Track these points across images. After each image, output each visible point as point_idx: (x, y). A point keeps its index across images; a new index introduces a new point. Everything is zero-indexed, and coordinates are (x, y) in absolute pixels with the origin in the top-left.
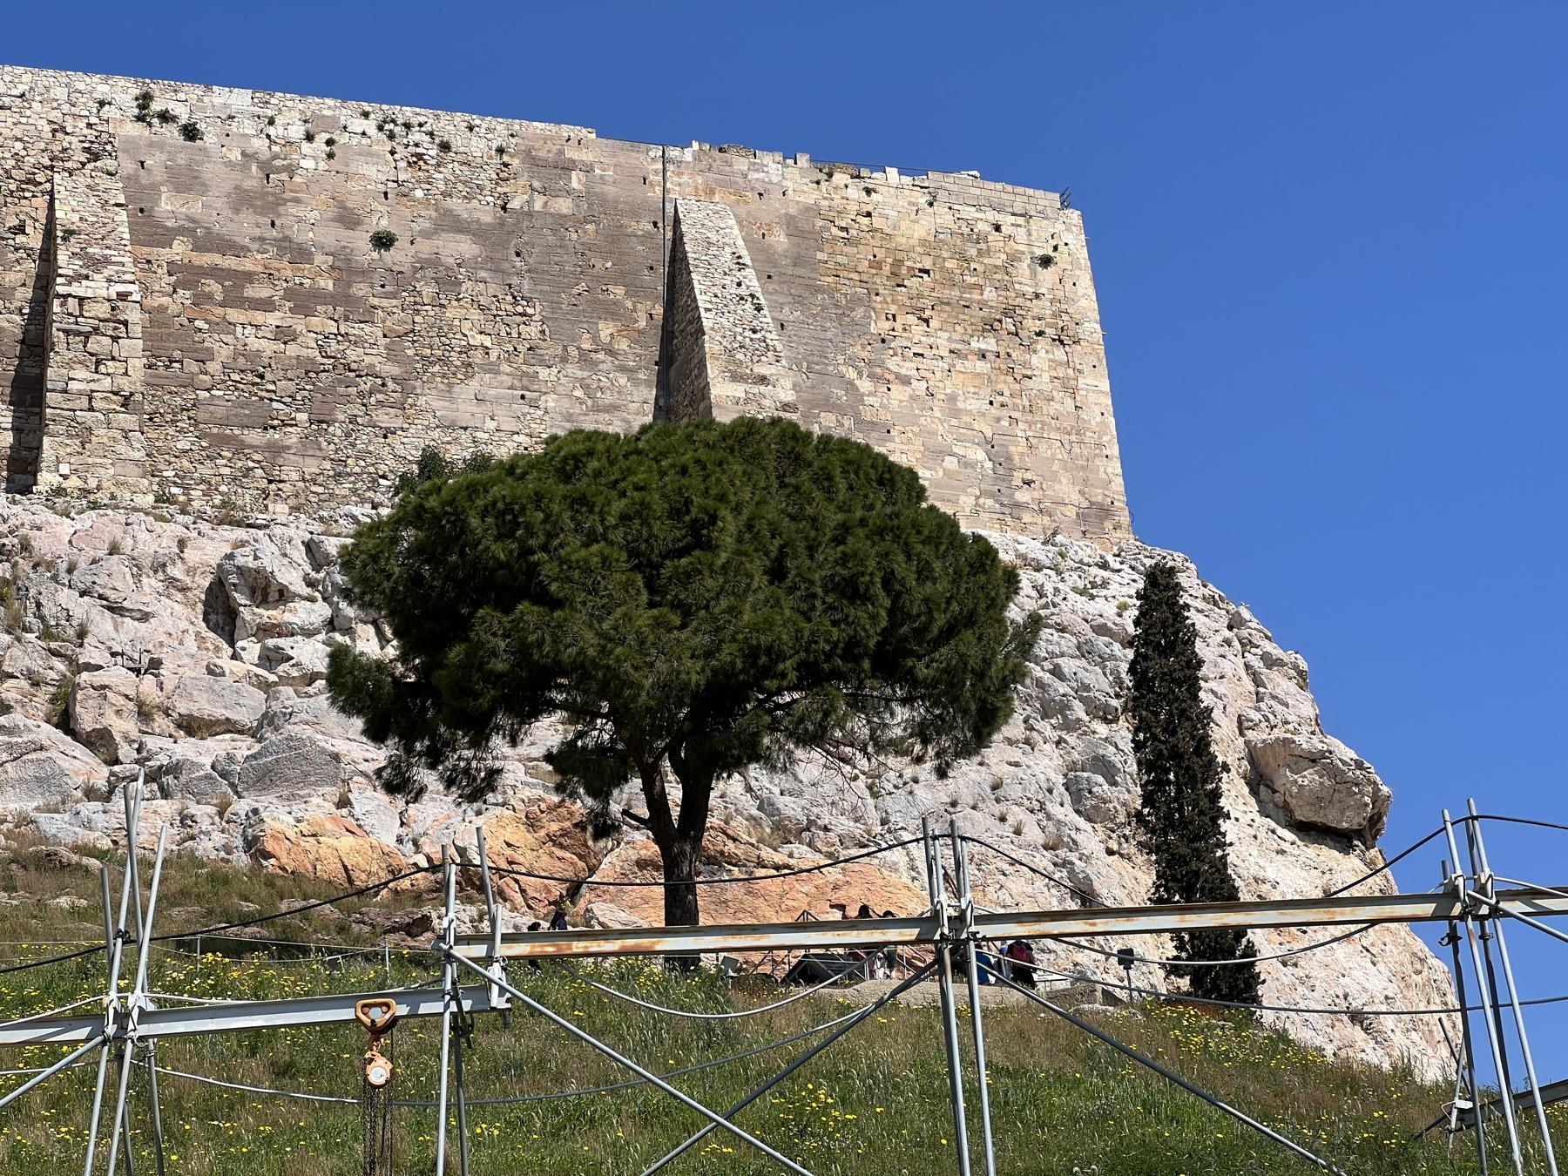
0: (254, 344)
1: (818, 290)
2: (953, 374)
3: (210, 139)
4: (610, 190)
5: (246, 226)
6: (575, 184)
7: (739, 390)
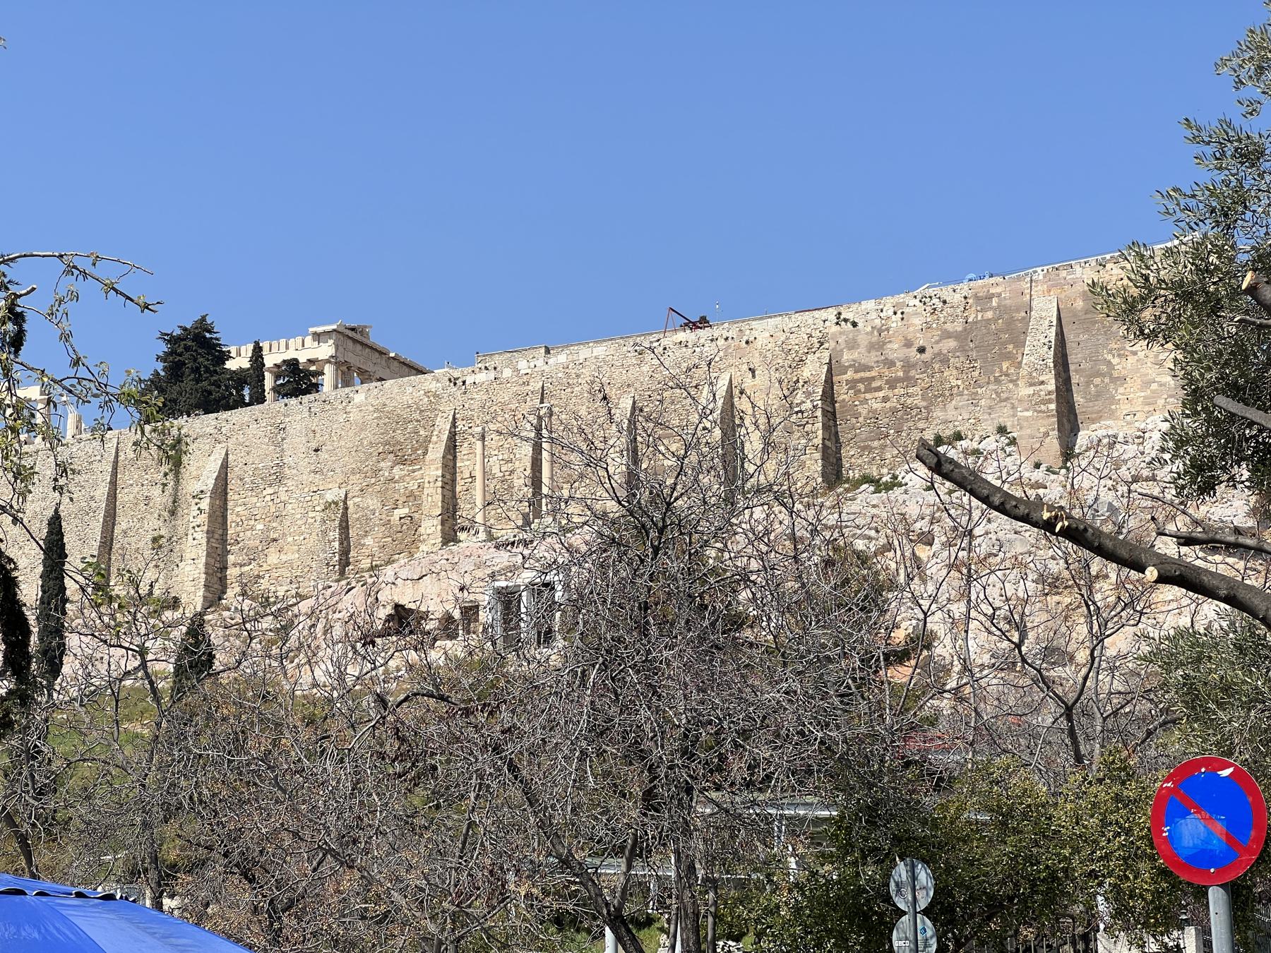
0: (875, 406)
1: (1096, 322)
3: (860, 325)
4: (1008, 302)
5: (873, 357)
6: (994, 304)
7: (1030, 391)
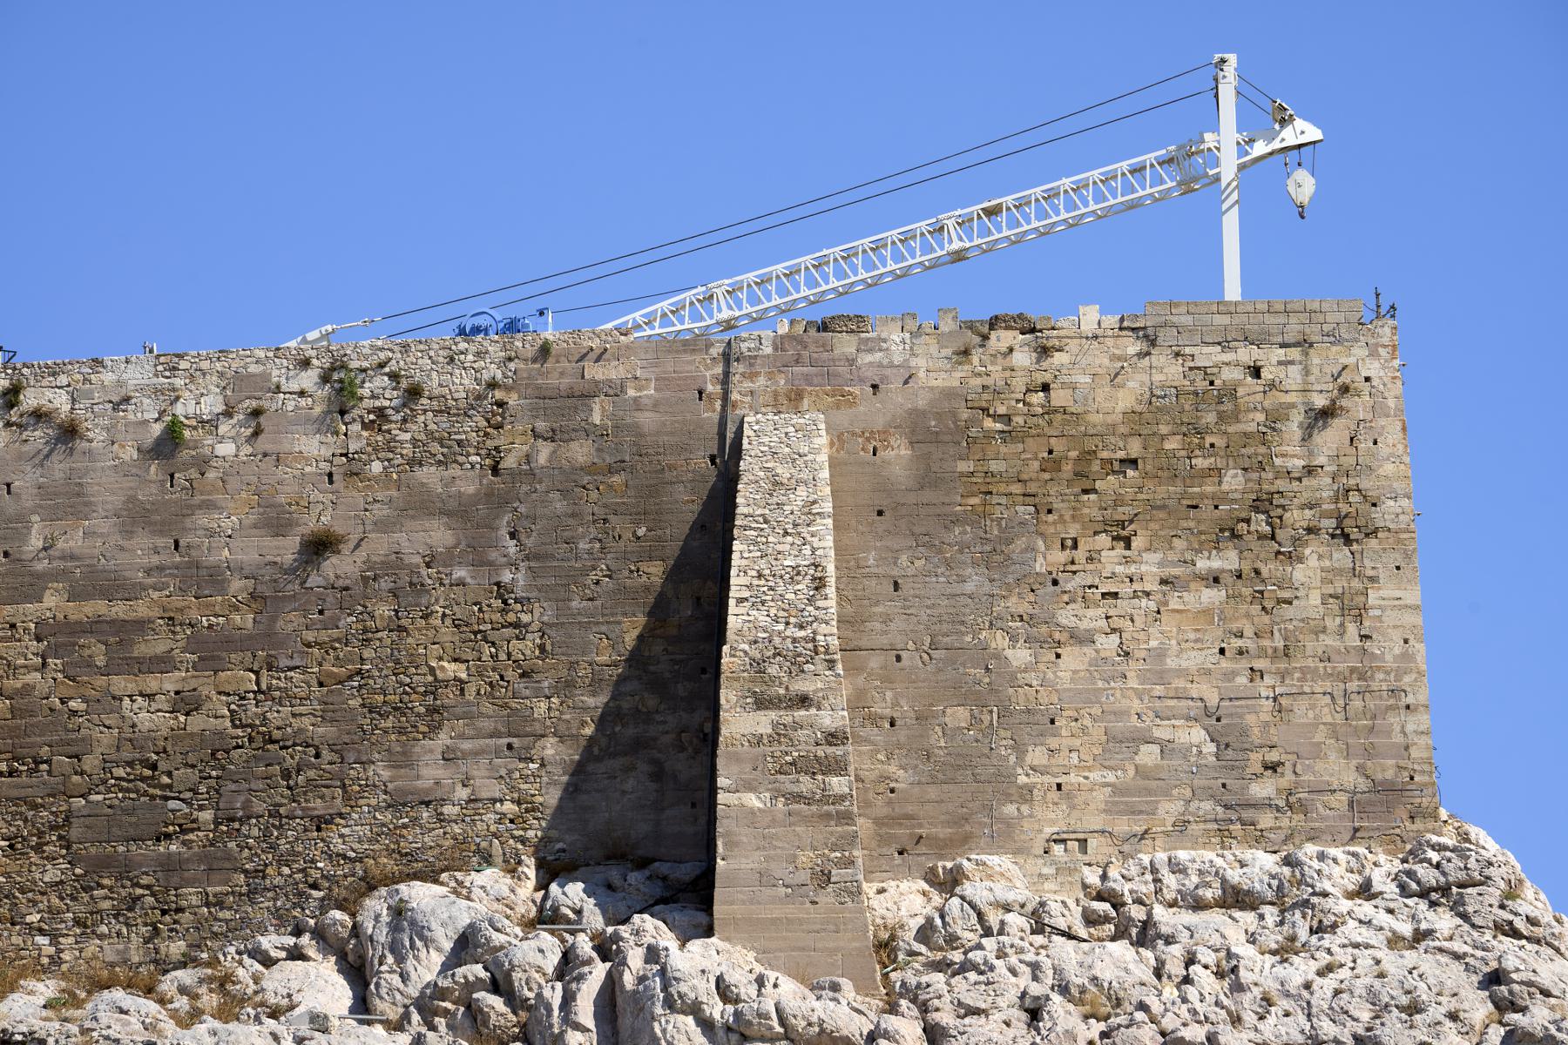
2: (1164, 617)
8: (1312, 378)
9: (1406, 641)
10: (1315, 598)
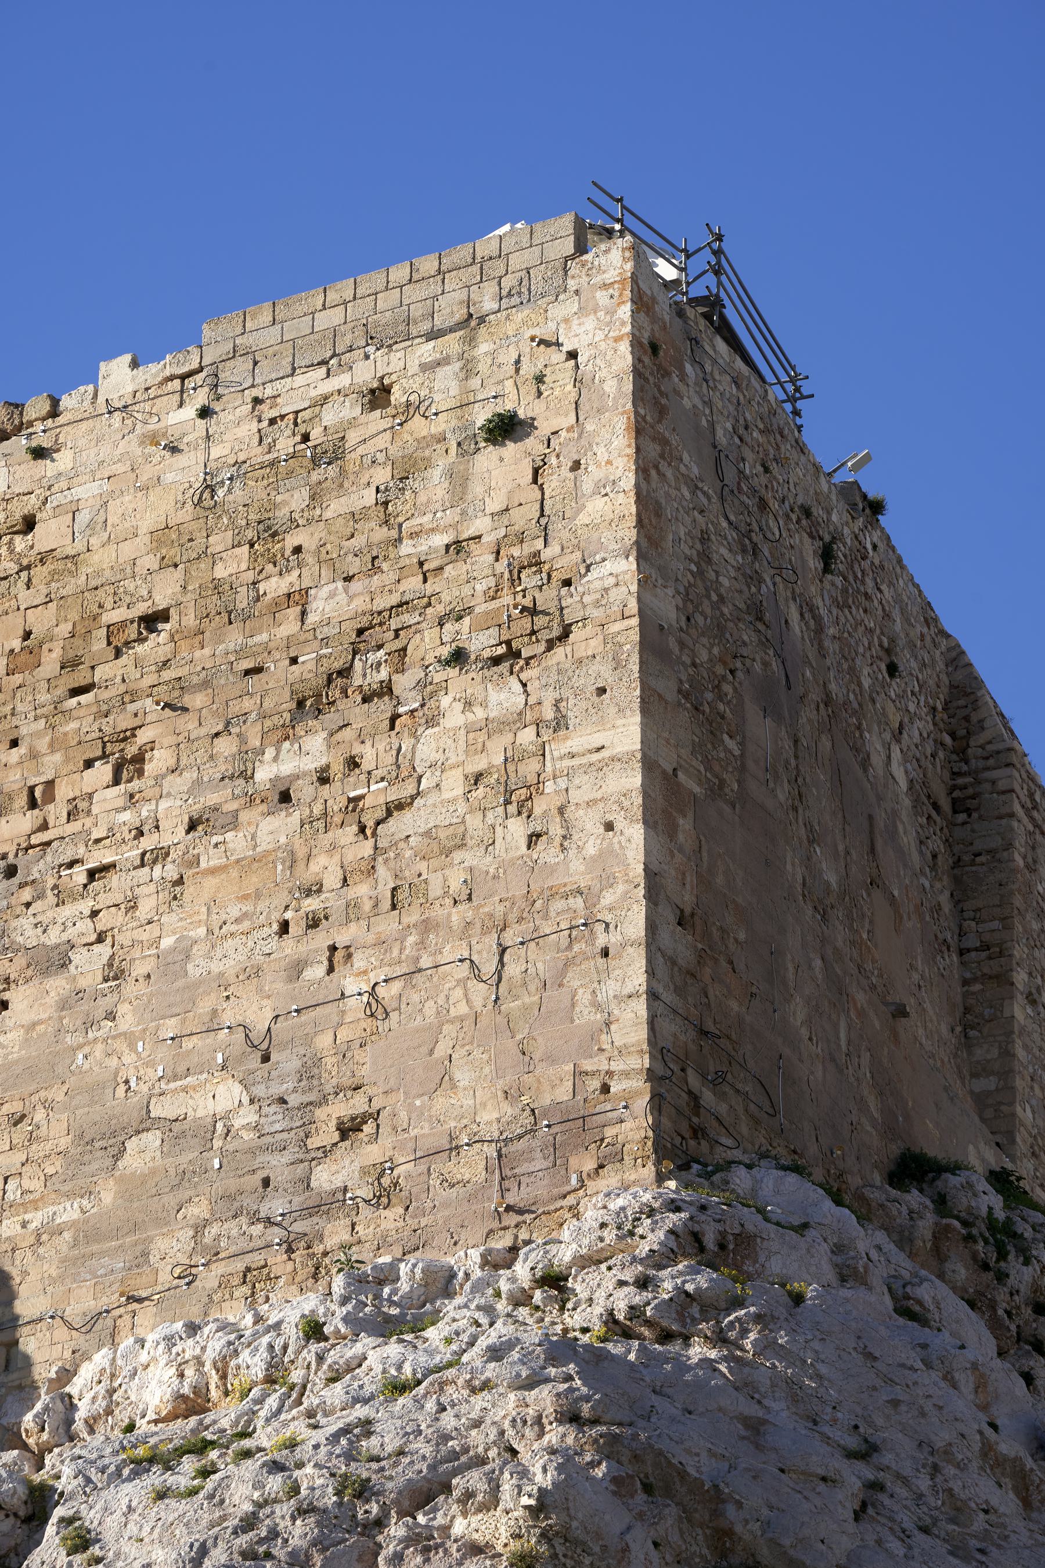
2: (189, 890)
8: (475, 383)
9: (609, 827)
10: (454, 785)
